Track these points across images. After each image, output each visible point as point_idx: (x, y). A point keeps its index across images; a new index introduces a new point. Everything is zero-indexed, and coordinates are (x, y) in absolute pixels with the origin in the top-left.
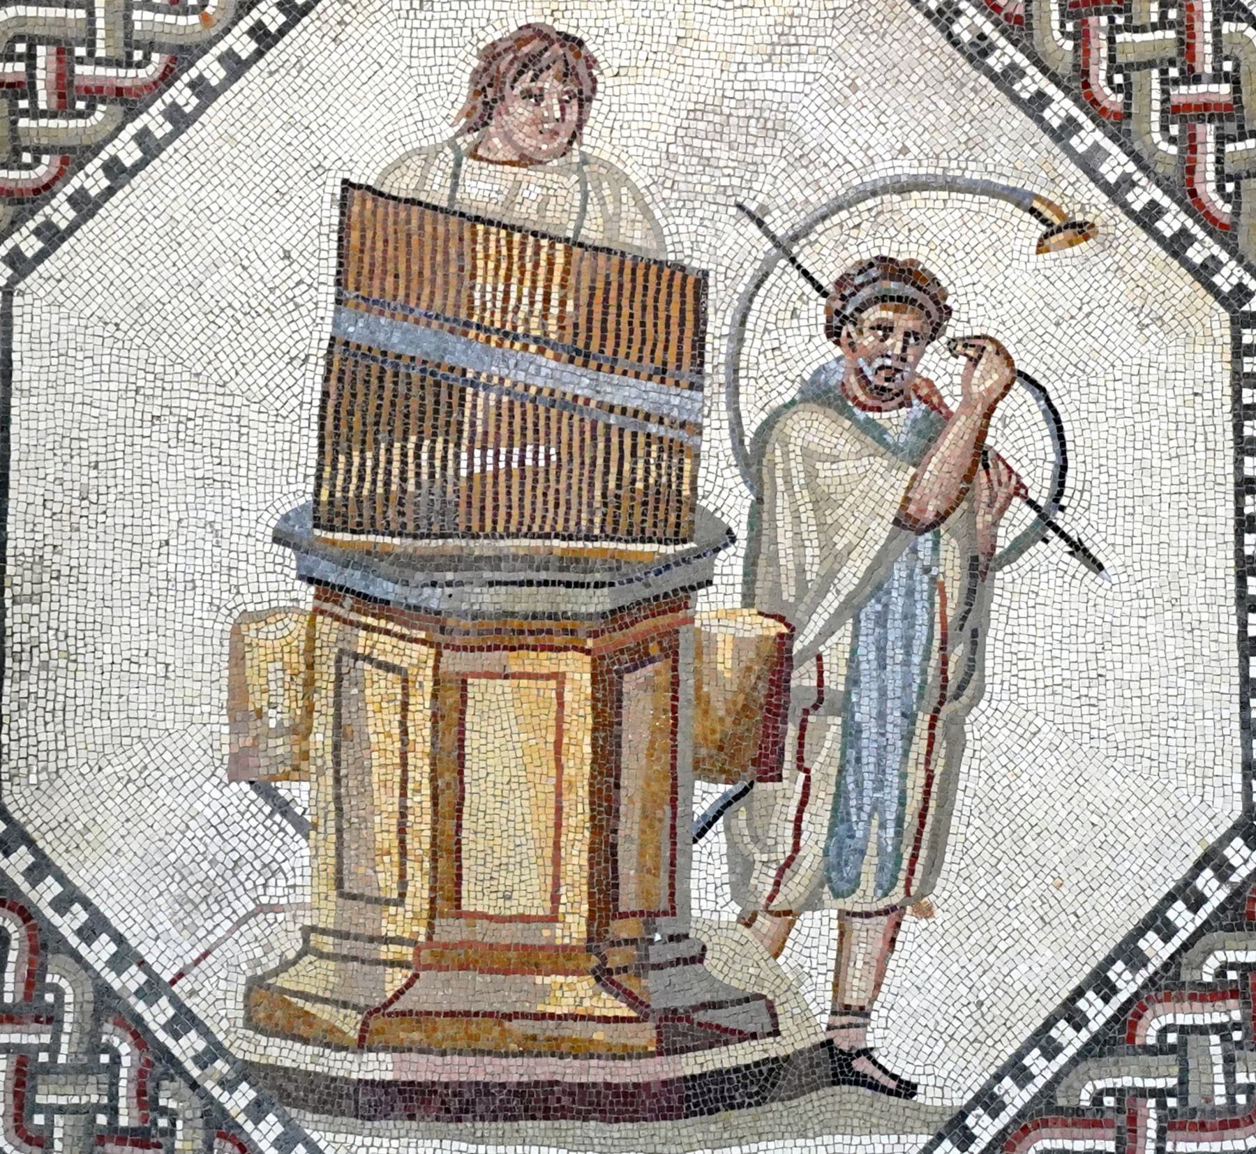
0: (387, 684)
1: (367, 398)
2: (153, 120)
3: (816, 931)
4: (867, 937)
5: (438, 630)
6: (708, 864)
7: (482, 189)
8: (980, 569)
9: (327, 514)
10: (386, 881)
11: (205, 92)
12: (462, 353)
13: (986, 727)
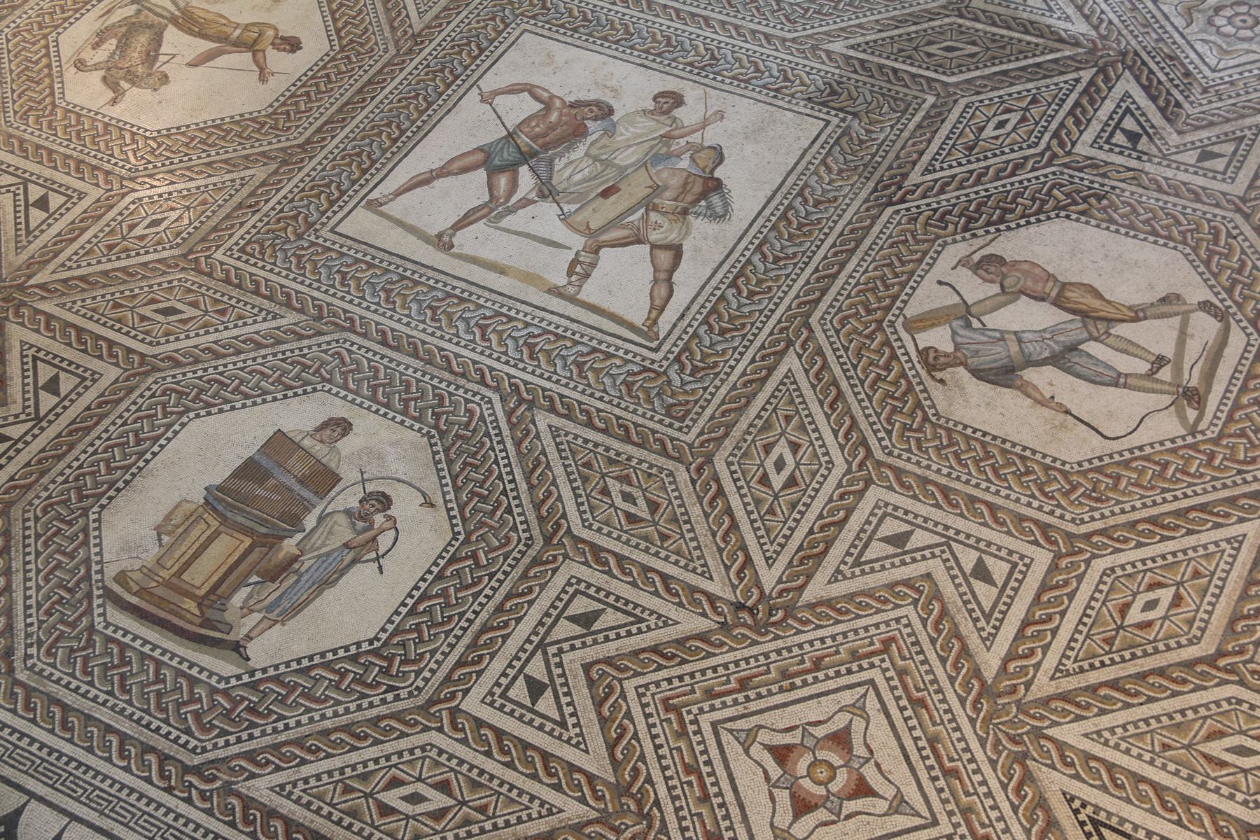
0: (204, 526)
1: (250, 470)
2: (249, 402)
3: (256, 617)
4: (266, 623)
5: (224, 520)
6: (244, 593)
7: (307, 443)
8: (354, 561)
9: (219, 488)
10: (169, 564)
11: (264, 401)
12: (277, 472)
13: (329, 594)
